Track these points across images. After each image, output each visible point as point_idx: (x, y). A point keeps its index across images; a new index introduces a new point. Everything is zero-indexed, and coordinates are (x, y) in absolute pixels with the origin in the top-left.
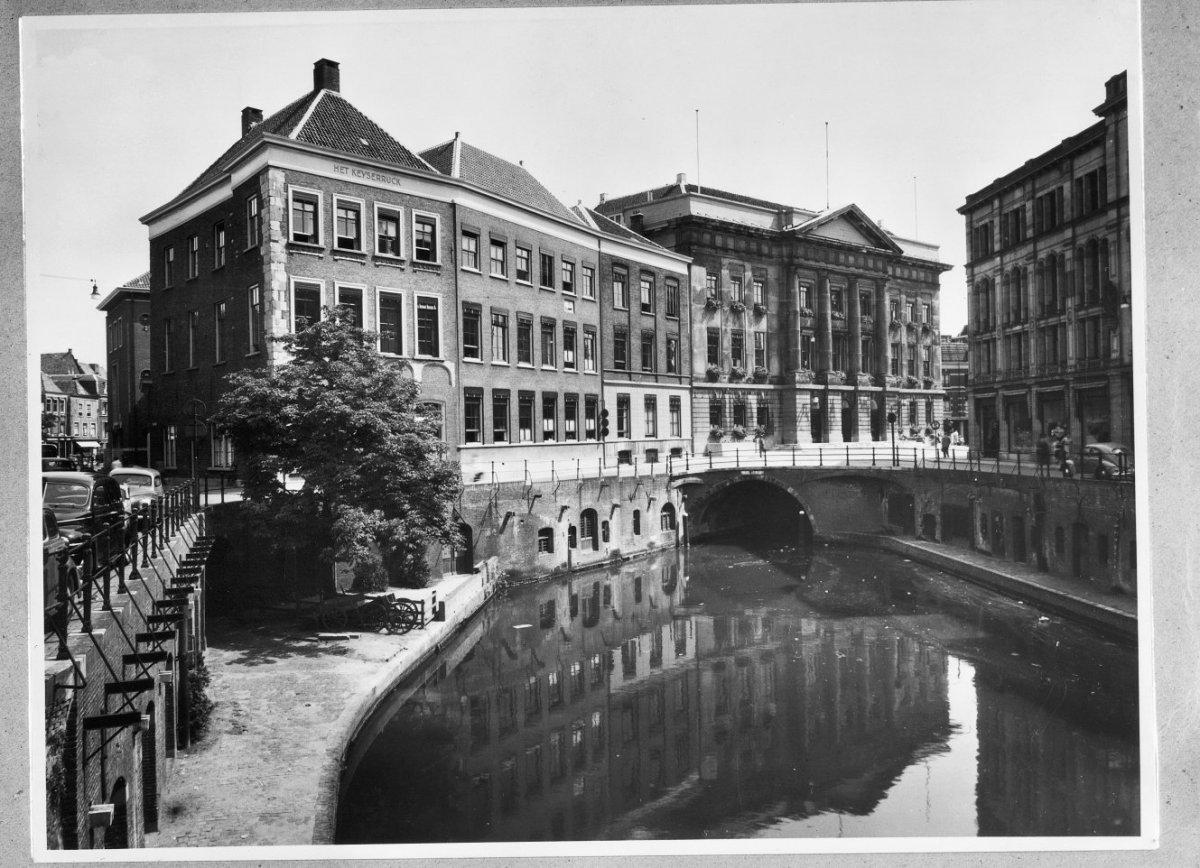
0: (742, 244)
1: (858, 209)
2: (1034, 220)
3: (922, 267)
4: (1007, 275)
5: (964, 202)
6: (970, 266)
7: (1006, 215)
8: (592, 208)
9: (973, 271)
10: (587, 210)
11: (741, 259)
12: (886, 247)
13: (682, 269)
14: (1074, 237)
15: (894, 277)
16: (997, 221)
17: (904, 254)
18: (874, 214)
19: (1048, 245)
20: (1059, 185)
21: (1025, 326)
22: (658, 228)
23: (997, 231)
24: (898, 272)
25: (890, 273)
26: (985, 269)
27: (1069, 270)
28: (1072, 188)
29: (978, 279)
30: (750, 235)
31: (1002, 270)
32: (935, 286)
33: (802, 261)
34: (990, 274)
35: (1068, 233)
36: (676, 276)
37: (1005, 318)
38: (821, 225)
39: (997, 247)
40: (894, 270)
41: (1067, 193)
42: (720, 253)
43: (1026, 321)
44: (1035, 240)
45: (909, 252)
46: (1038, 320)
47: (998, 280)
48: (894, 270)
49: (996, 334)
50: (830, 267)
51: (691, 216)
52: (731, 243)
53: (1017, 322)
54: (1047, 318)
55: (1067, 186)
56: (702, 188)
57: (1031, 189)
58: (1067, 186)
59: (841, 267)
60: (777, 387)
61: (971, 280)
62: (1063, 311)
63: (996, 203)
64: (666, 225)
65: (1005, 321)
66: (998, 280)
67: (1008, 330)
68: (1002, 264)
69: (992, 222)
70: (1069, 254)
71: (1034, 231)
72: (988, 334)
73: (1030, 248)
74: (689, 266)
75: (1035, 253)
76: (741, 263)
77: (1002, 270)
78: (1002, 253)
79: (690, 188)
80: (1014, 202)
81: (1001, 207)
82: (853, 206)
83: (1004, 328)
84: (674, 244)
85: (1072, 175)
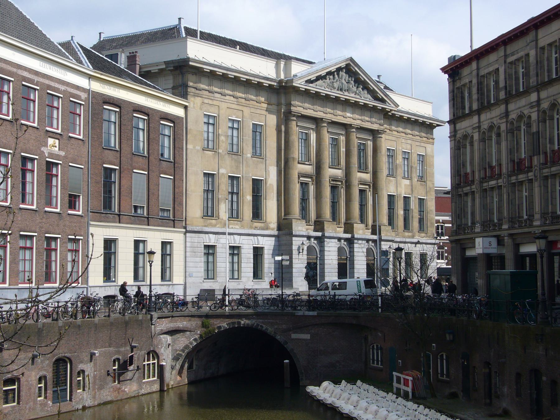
2: (506, 83)
5: (446, 63)
8: (88, 46)
9: (455, 127)
10: (82, 47)
12: (383, 101)
13: (179, 112)
14: (539, 101)
16: (475, 81)
17: (400, 108)
19: (517, 106)
20: (526, 52)
21: (500, 181)
22: (154, 69)
23: (474, 90)
26: (464, 125)
27: (535, 131)
28: (536, 54)
29: (459, 135)
31: (479, 127)
34: (469, 131)
35: (534, 97)
36: (172, 119)
37: (482, 172)
41: (532, 59)
43: (500, 175)
44: (506, 102)
46: (510, 176)
47: (476, 136)
51: (188, 60)
53: (492, 178)
54: (517, 175)
57: (503, 54)
58: (532, 53)
59: (339, 117)
61: (453, 135)
63: (474, 65)
64: (164, 67)
65: (482, 175)
66: (476, 136)
67: (485, 184)
68: (479, 122)
69: (471, 82)
71: (506, 94)
72: (469, 188)
74: (186, 107)
75: (507, 114)
78: (479, 112)
79: (191, 33)
80: (489, 65)
81: (478, 69)
82: (351, 59)
83: (481, 182)
84: (171, 86)
85: (537, 44)
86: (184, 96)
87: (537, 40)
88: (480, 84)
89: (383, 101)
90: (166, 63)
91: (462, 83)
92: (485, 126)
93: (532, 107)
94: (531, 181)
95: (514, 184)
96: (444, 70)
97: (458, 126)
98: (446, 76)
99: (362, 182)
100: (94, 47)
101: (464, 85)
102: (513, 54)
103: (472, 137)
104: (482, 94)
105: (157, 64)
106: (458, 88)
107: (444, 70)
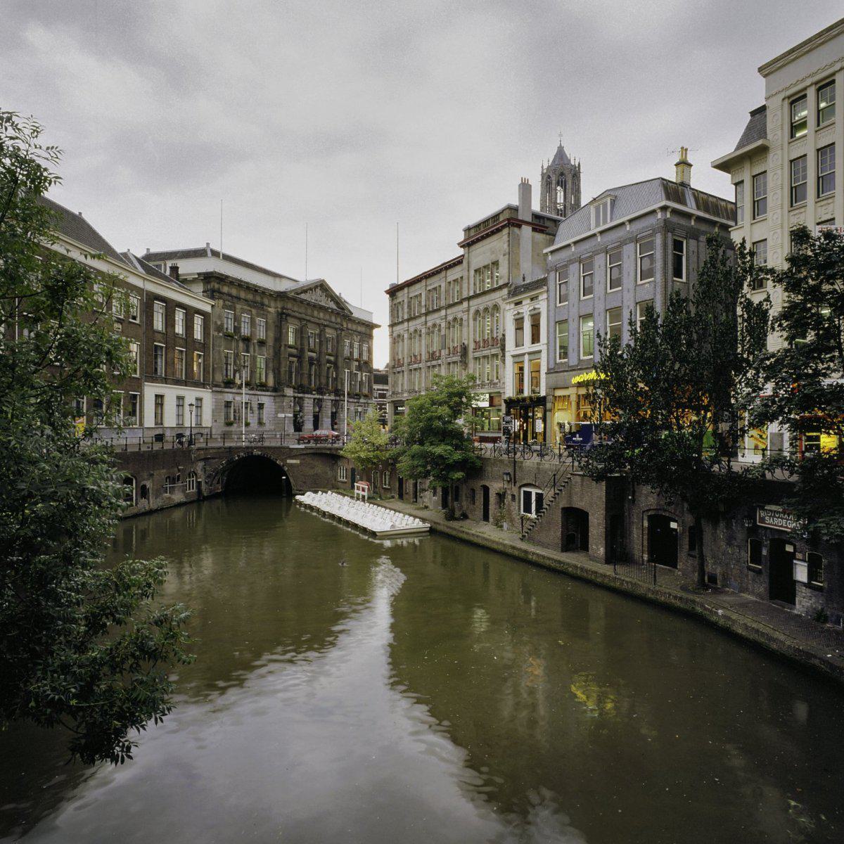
0: (250, 297)
1: (326, 283)
3: (364, 324)
4: (411, 334)
5: (388, 288)
6: (392, 325)
7: (411, 298)
8: (139, 256)
11: (249, 306)
13: (208, 309)
15: (348, 329)
16: (406, 301)
18: (337, 289)
22: (190, 278)
23: (406, 306)
24: (350, 326)
25: (345, 326)
26: (398, 329)
29: (395, 335)
30: (256, 291)
31: (408, 330)
32: (370, 337)
33: (290, 312)
34: (402, 332)
37: (409, 358)
38: (305, 291)
39: (406, 317)
40: (347, 324)
41: (443, 289)
42: (235, 300)
45: (356, 315)
46: (426, 361)
47: (406, 336)
48: (347, 324)
49: (404, 368)
50: (308, 318)
52: (243, 295)
53: (415, 363)
55: (443, 285)
56: (223, 255)
58: (443, 285)
60: (274, 394)
62: (439, 358)
63: (406, 290)
64: (197, 276)
66: (406, 336)
69: (403, 301)
70: (443, 325)
73: (423, 319)
74: (213, 306)
75: (426, 322)
76: (249, 308)
77: (408, 330)
79: (215, 254)
82: (323, 281)
83: (409, 365)
86: (212, 298)
87: (446, 277)
88: (409, 303)
89: (343, 309)
90: (199, 274)
91: (398, 301)
92: (412, 330)
93: (442, 319)
94: (440, 365)
95: (429, 367)
96: (387, 292)
97: (395, 328)
98: (388, 296)
99: (329, 362)
100: (143, 258)
101: (400, 303)
102: (431, 285)
103: (403, 336)
104: (410, 309)
105: (193, 274)
106: (395, 305)
107: (387, 292)
